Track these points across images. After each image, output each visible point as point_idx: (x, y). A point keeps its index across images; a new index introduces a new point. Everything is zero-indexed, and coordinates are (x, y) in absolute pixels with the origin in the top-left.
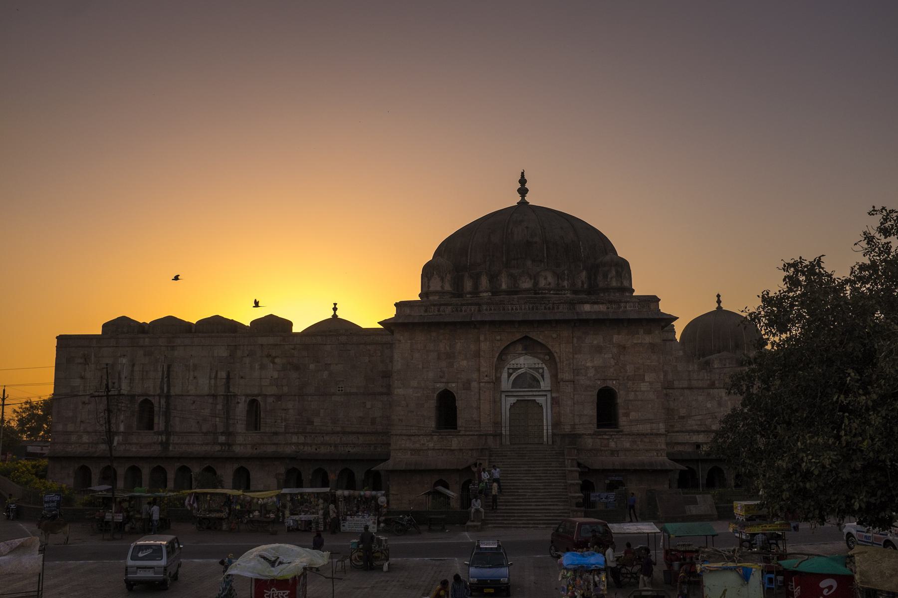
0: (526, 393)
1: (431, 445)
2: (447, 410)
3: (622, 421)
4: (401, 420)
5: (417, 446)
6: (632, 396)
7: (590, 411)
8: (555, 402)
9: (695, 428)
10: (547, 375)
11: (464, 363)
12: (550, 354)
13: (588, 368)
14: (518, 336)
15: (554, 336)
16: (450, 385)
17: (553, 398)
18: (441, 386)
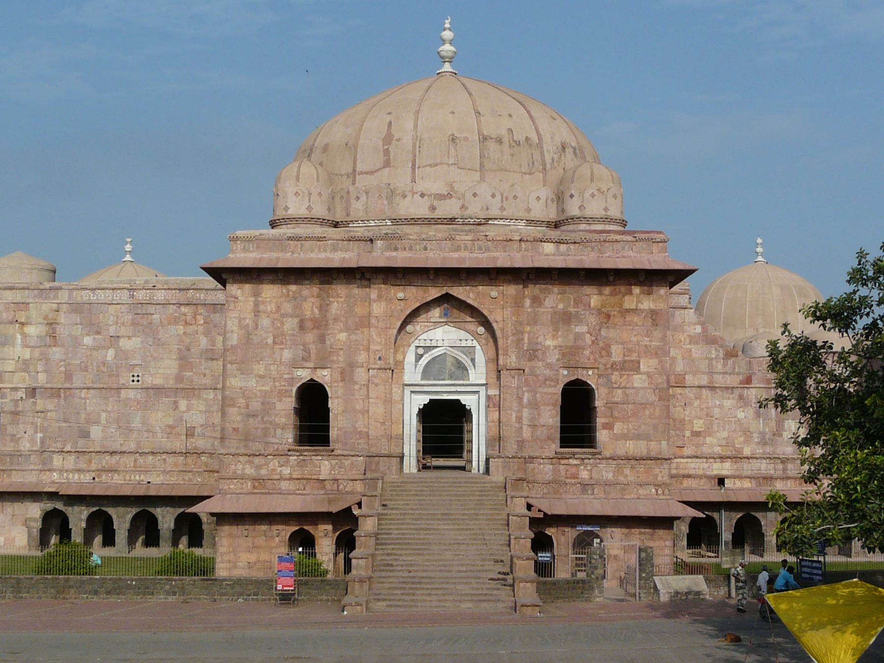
0: (445, 391)
1: (286, 471)
3: (602, 435)
5: (264, 472)
6: (618, 395)
7: (551, 418)
8: (494, 403)
9: (718, 450)
11: (343, 336)
12: (486, 323)
13: (548, 348)
14: (434, 293)
17: (488, 397)
18: (304, 375)
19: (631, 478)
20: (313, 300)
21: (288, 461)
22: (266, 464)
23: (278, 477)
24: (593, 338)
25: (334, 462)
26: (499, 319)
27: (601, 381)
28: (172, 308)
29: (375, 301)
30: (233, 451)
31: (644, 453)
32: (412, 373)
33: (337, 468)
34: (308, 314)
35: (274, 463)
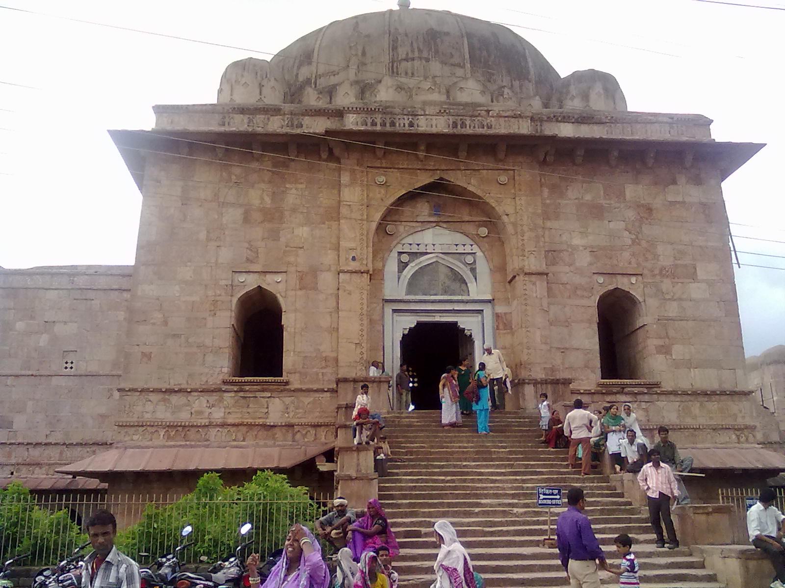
1: (218, 415)
2: (259, 340)
3: (655, 364)
4: (147, 356)
5: (184, 416)
6: (672, 310)
7: (588, 340)
10: (483, 267)
11: (303, 232)
13: (575, 248)
14: (425, 179)
15: (503, 179)
16: (269, 278)
17: (497, 316)
18: (251, 282)
19: (702, 421)
20: (263, 186)
21: (221, 400)
22: (189, 404)
23: (205, 422)
24: (634, 237)
25: (288, 400)
26: (510, 210)
27: (647, 291)
28: (114, 295)
29: (346, 186)
30: (140, 385)
31: (715, 386)
32: (394, 286)
33: (292, 408)
34: (256, 202)
35: (200, 403)
